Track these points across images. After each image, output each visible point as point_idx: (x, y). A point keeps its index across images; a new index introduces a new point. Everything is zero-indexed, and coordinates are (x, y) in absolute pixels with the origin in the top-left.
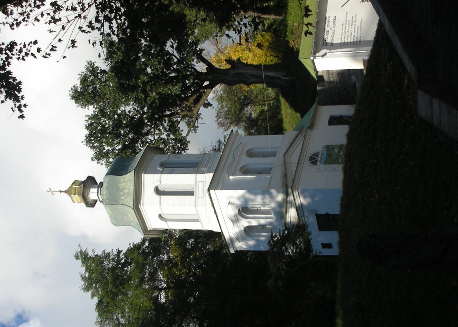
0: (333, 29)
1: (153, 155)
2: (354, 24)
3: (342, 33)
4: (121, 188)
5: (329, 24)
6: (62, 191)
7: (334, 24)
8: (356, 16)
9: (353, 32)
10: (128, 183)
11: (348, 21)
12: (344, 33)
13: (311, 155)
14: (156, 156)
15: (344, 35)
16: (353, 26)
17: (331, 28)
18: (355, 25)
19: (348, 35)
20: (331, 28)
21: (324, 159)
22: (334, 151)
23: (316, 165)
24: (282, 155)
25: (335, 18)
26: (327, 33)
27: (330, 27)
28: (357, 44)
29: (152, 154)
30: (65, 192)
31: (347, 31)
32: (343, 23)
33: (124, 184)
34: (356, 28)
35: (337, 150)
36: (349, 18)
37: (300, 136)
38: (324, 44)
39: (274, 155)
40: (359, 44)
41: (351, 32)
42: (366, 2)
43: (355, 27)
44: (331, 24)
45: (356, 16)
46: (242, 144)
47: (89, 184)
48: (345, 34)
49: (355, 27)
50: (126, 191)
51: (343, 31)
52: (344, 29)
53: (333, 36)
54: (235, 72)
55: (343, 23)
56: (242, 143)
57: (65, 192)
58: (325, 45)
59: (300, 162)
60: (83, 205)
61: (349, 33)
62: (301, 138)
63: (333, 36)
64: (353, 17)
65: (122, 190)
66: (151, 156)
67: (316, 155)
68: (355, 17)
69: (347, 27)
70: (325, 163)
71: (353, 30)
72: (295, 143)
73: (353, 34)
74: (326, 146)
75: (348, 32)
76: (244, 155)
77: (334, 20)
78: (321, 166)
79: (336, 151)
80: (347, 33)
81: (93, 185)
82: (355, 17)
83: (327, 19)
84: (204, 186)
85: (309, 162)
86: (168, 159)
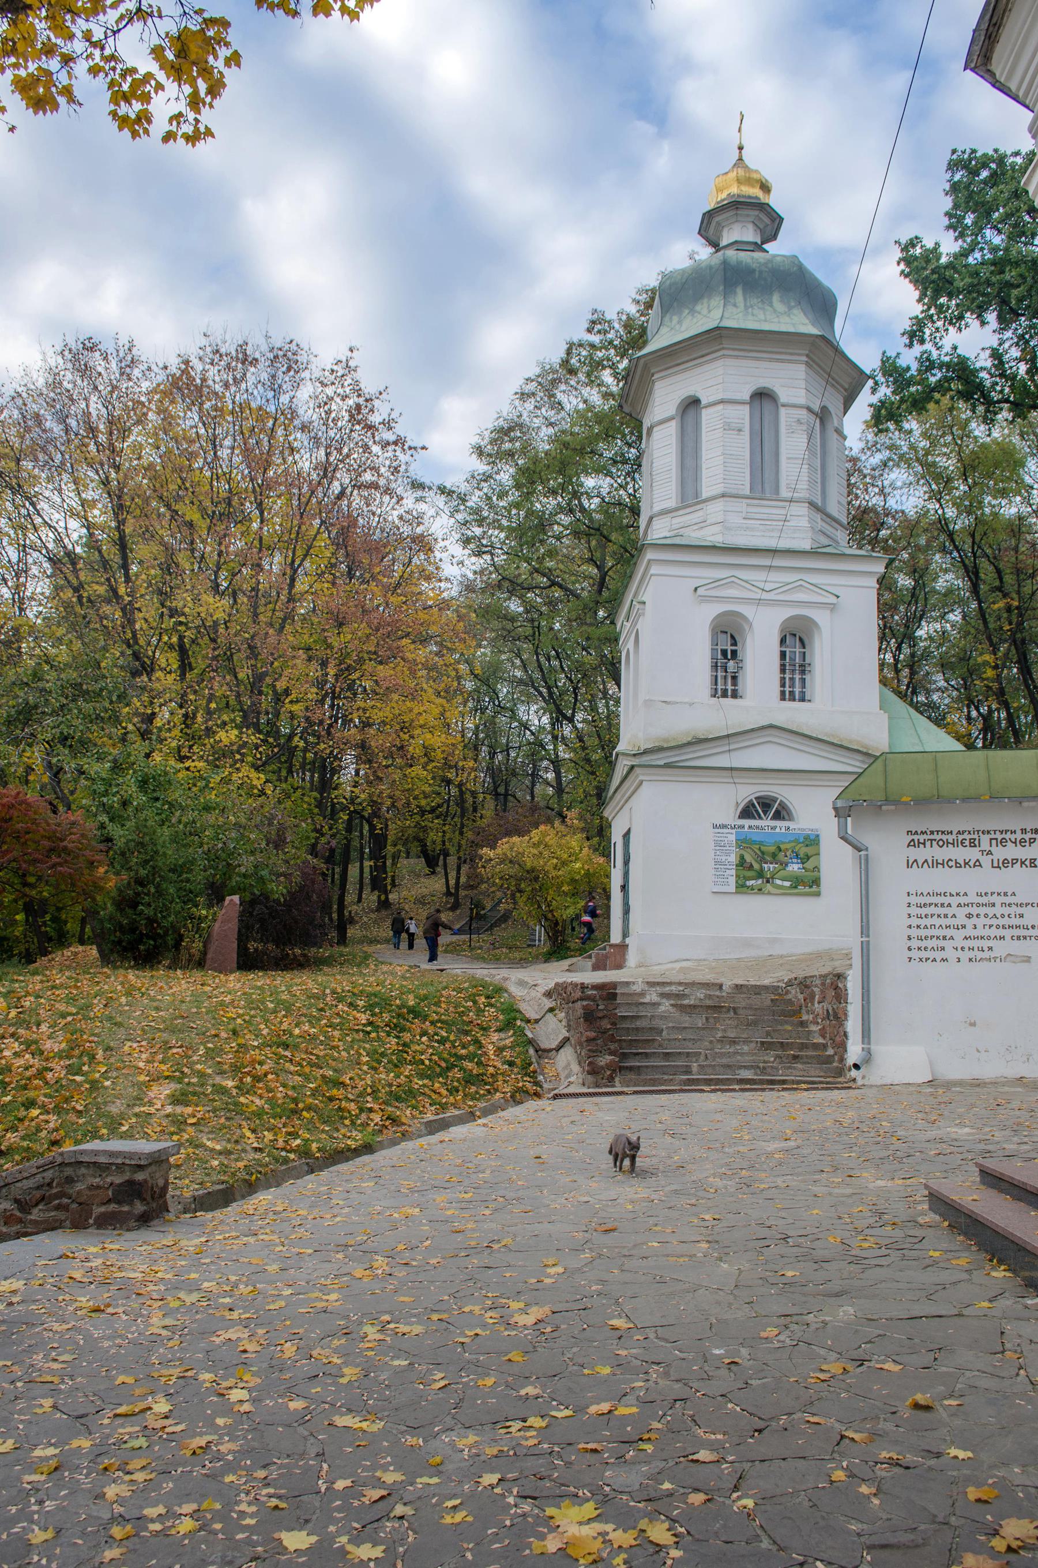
0: (986, 860)
1: (804, 358)
3: (966, 894)
4: (698, 308)
5: (1009, 844)
6: (743, 151)
9: (969, 931)
11: (1019, 910)
12: (962, 900)
13: (780, 798)
14: (803, 367)
16: (994, 931)
18: (1002, 938)
19: (954, 916)
20: (990, 853)
22: (795, 860)
26: (967, 843)
27: (994, 849)
28: (909, 949)
29: (807, 356)
30: (740, 159)
31: (974, 911)
32: (1014, 894)
33: (705, 311)
34: (985, 944)
35: (796, 869)
37: (860, 757)
38: (916, 837)
41: (970, 926)
43: (989, 938)
47: (748, 216)
48: (959, 905)
49: (989, 938)
51: (972, 898)
52: (984, 900)
53: (950, 863)
55: (1014, 894)
56: (838, 597)
57: (740, 159)
58: (913, 840)
59: (735, 773)
61: (961, 920)
63: (950, 863)
66: (799, 355)
67: (782, 813)
69: (991, 911)
70: (743, 843)
71: (975, 933)
74: (818, 836)
75: (969, 916)
77: (1027, 863)
79: (794, 868)
81: (751, 227)
84: (695, 527)
85: (752, 797)
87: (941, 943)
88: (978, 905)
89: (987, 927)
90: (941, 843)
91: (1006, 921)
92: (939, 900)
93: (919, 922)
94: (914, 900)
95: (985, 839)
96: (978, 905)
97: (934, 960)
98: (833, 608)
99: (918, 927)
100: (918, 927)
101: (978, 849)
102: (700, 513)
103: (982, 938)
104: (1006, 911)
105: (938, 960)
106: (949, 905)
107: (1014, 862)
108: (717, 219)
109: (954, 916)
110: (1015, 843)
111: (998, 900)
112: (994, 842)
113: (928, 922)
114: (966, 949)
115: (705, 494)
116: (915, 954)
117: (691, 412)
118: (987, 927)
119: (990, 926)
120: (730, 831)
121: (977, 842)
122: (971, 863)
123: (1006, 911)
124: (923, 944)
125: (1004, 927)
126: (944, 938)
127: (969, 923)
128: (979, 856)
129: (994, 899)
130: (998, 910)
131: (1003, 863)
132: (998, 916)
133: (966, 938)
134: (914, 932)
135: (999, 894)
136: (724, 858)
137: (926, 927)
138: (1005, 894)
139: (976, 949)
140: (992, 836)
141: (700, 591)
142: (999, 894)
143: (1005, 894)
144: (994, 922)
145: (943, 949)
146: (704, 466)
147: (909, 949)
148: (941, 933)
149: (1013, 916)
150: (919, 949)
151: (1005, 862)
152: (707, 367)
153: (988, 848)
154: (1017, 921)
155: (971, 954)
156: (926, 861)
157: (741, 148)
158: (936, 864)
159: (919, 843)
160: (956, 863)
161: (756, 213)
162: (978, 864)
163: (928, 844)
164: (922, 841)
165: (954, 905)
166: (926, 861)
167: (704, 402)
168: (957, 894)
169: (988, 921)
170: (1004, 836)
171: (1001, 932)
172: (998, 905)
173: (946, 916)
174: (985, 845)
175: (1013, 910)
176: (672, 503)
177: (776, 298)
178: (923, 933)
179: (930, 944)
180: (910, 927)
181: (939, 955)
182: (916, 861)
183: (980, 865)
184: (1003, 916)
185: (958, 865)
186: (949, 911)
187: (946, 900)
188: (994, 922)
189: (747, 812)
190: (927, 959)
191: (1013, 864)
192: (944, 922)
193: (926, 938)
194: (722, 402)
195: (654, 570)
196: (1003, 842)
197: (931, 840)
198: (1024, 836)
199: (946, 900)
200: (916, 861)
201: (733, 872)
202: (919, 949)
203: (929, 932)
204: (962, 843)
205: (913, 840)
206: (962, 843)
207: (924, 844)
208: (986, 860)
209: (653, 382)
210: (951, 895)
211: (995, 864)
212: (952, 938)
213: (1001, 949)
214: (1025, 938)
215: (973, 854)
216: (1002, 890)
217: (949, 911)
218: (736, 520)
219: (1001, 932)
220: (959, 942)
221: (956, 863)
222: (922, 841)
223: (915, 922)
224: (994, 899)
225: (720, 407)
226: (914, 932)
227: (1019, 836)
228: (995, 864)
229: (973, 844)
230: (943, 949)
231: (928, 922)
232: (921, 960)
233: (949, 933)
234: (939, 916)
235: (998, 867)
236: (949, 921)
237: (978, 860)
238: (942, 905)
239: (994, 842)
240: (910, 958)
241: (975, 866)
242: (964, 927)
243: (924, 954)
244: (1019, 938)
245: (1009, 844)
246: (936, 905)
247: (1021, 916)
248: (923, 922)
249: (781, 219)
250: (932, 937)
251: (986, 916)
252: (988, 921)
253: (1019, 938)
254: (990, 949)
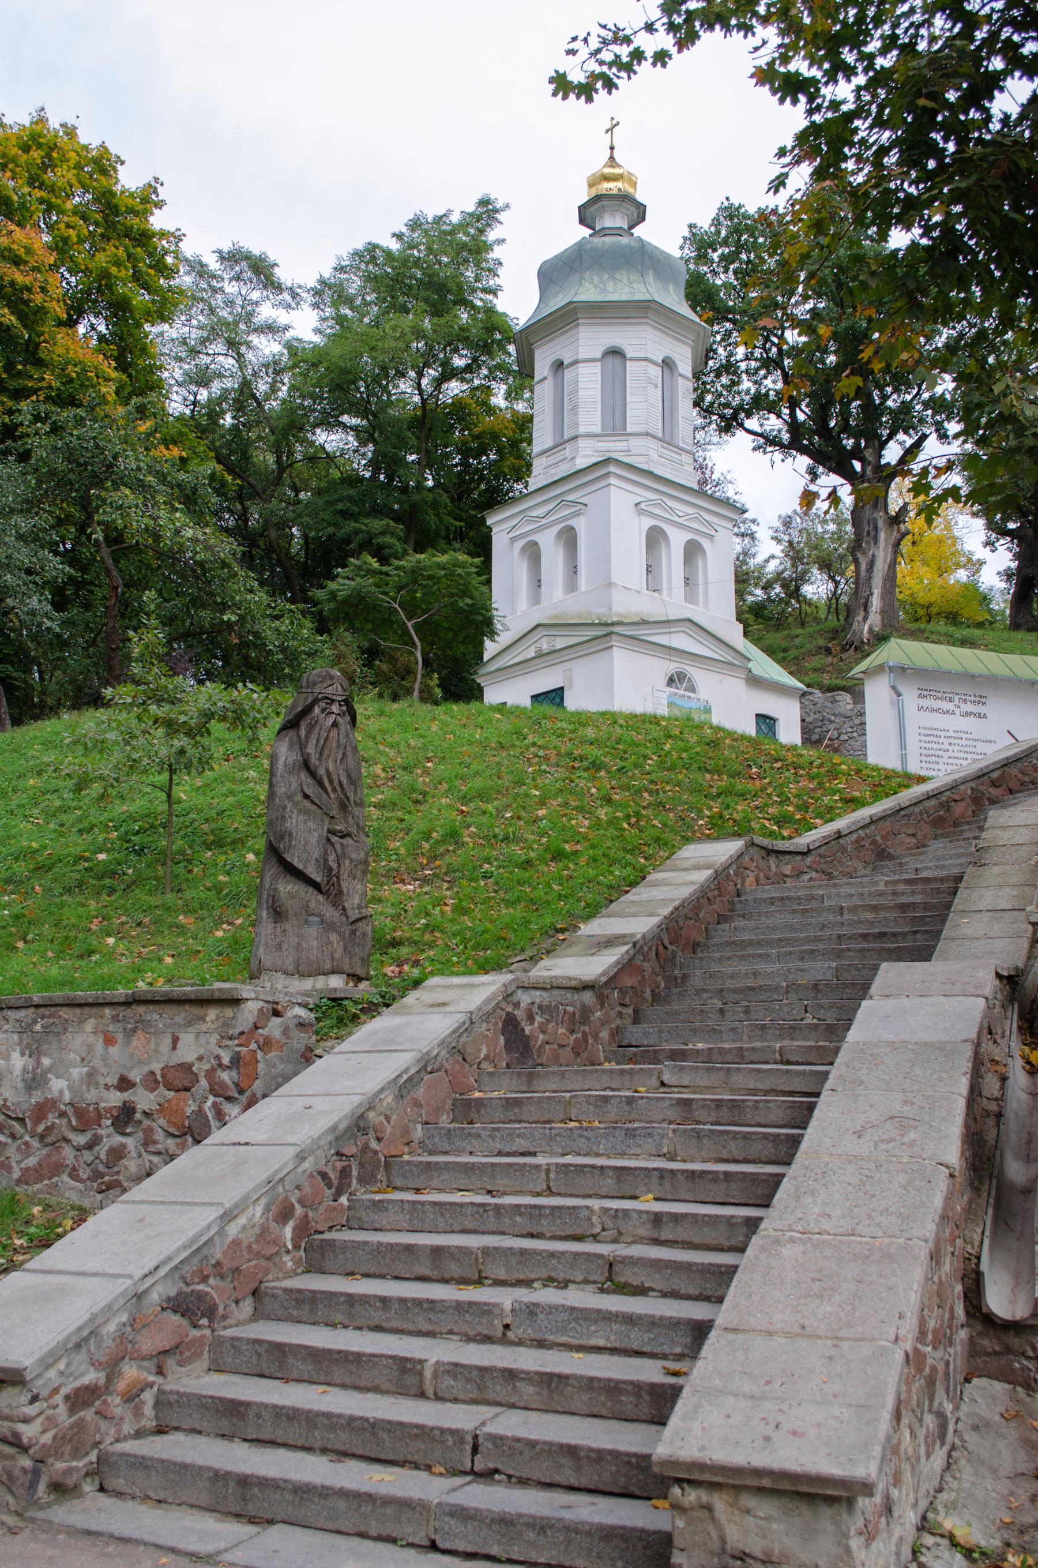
0: (957, 711)
4: (618, 276)
7: (967, 714)
9: (950, 754)
10: (627, 289)
15: (943, 734)
16: (962, 755)
21: (680, 702)
23: (668, 685)
24: (688, 615)
30: (612, 158)
31: (953, 741)
33: (625, 280)
37: (732, 653)
39: (691, 597)
46: (713, 533)
50: (610, 286)
54: (881, 524)
57: (612, 158)
60: (585, 199)
61: (946, 746)
62: (728, 657)
65: (612, 277)
67: (692, 689)
72: (716, 643)
73: (946, 755)
76: (690, 536)
78: (665, 695)
80: (946, 741)
86: (681, 375)
95: (957, 698)
98: (711, 537)
102: (625, 444)
104: (968, 743)
108: (604, 203)
111: (964, 736)
115: (629, 430)
117: (610, 359)
123: (968, 743)
127: (950, 748)
130: (964, 742)
134: (923, 751)
141: (642, 506)
146: (628, 407)
152: (629, 328)
154: (973, 750)
157: (612, 148)
158: (933, 710)
161: (633, 209)
162: (953, 713)
167: (628, 356)
174: (956, 702)
175: (971, 743)
176: (597, 429)
177: (671, 288)
179: (932, 759)
187: (939, 733)
189: (671, 681)
194: (646, 359)
195: (612, 480)
196: (965, 701)
199: (939, 733)
208: (957, 711)
209: (578, 325)
215: (950, 706)
218: (654, 455)
223: (923, 745)
225: (644, 363)
226: (923, 751)
227: (972, 698)
229: (951, 700)
233: (940, 753)
248: (928, 746)
249: (643, 219)
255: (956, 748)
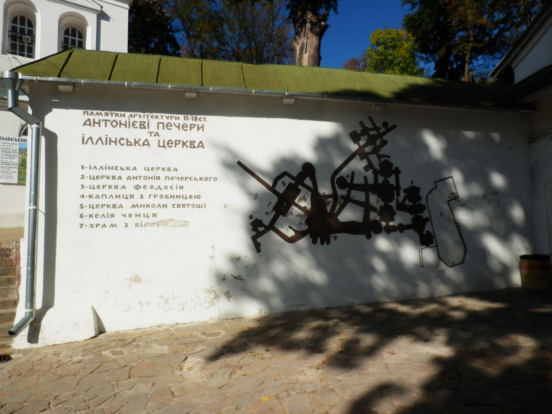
0: (153, 141)
2: (170, 202)
3: (135, 168)
5: (173, 127)
8: (199, 206)
9: (137, 200)
11: (180, 183)
12: (132, 173)
15: (124, 174)
16: (158, 201)
17: (157, 134)
19: (124, 187)
20: (157, 134)
25: (196, 144)
26: (138, 125)
27: (160, 131)
28: (81, 216)
31: (142, 183)
34: (150, 211)
36: (190, 188)
40: (82, 225)
42: (254, 233)
43: (153, 206)
44: (175, 134)
45: (199, 206)
48: (129, 178)
49: (153, 206)
51: (141, 172)
52: (151, 174)
53: (122, 142)
55: (176, 169)
58: (89, 120)
61: (130, 190)
64: (198, 197)
68: (193, 206)
69: (156, 183)
71: (142, 202)
77: (188, 144)
82: (193, 206)
83: (194, 122)
87: (111, 211)
88: (145, 178)
89: (152, 197)
90: (114, 124)
91: (169, 192)
92: (110, 173)
93: (92, 192)
94: (87, 172)
96: (145, 178)
97: (104, 226)
99: (90, 196)
100: (90, 196)
101: (147, 130)
103: (147, 206)
104: (169, 183)
105: (108, 225)
106: (120, 178)
107: (177, 143)
109: (124, 187)
110: (179, 127)
112: (161, 125)
113: (100, 192)
114: (134, 216)
116: (86, 221)
118: (152, 197)
119: (155, 196)
120: (15, 142)
121: (146, 125)
122: (141, 143)
123: (169, 183)
124: (94, 212)
125: (166, 197)
126: (114, 206)
127: (137, 193)
128: (148, 136)
129: (160, 173)
130: (162, 183)
131: (168, 143)
132: (162, 187)
133: (133, 206)
134: (86, 201)
135: (163, 169)
136: (9, 160)
137: (98, 197)
138: (169, 169)
139: (142, 215)
140: (160, 120)
142: (163, 169)
143: (169, 169)
144: (159, 192)
145: (113, 216)
147: (81, 216)
148: (111, 202)
149: (174, 187)
150: (90, 216)
151: (170, 142)
153: (155, 130)
155: (138, 220)
156: (100, 138)
159: (94, 122)
160: (127, 141)
162: (146, 143)
163: (103, 124)
164: (97, 121)
165: (124, 177)
166: (100, 138)
168: (127, 168)
169: (153, 192)
170: (169, 120)
171: (164, 201)
172: (162, 178)
173: (116, 187)
174: (153, 127)
175: (175, 182)
178: (94, 202)
179: (100, 211)
180: (83, 196)
181: (108, 221)
182: (91, 138)
183: (148, 144)
184: (166, 187)
185: (129, 143)
186: (120, 183)
188: (159, 192)
190: (97, 225)
191: (176, 144)
192: (114, 192)
193: (97, 206)
197: (106, 121)
198: (186, 122)
200: (91, 138)
201: (17, 170)
202: (90, 216)
203: (100, 201)
204: (133, 125)
205: (89, 120)
206: (133, 125)
207: (99, 123)
208: (153, 141)
210: (122, 169)
211: (161, 144)
212: (121, 206)
213: (163, 215)
214: (184, 206)
215: (142, 135)
216: (166, 167)
217: (120, 183)
219: (164, 201)
220: (127, 210)
221: (127, 141)
222: (97, 121)
223: (87, 192)
224: (160, 173)
228: (161, 144)
229: (142, 126)
230: (113, 216)
231: (100, 192)
232: (92, 226)
233: (118, 202)
234: (110, 187)
235: (164, 146)
236: (119, 192)
237: (146, 140)
238: (114, 178)
239: (161, 125)
240: (82, 225)
241: (144, 144)
242: (132, 196)
243: (94, 221)
244: (178, 206)
245: (173, 127)
246: (108, 177)
247: (181, 188)
248: (95, 192)
250: (103, 206)
251: (152, 187)
252: (153, 192)
253: (178, 206)
254: (154, 215)
255: (146, 193)
